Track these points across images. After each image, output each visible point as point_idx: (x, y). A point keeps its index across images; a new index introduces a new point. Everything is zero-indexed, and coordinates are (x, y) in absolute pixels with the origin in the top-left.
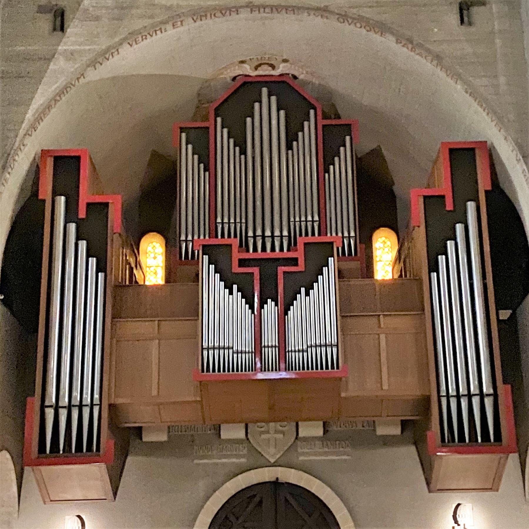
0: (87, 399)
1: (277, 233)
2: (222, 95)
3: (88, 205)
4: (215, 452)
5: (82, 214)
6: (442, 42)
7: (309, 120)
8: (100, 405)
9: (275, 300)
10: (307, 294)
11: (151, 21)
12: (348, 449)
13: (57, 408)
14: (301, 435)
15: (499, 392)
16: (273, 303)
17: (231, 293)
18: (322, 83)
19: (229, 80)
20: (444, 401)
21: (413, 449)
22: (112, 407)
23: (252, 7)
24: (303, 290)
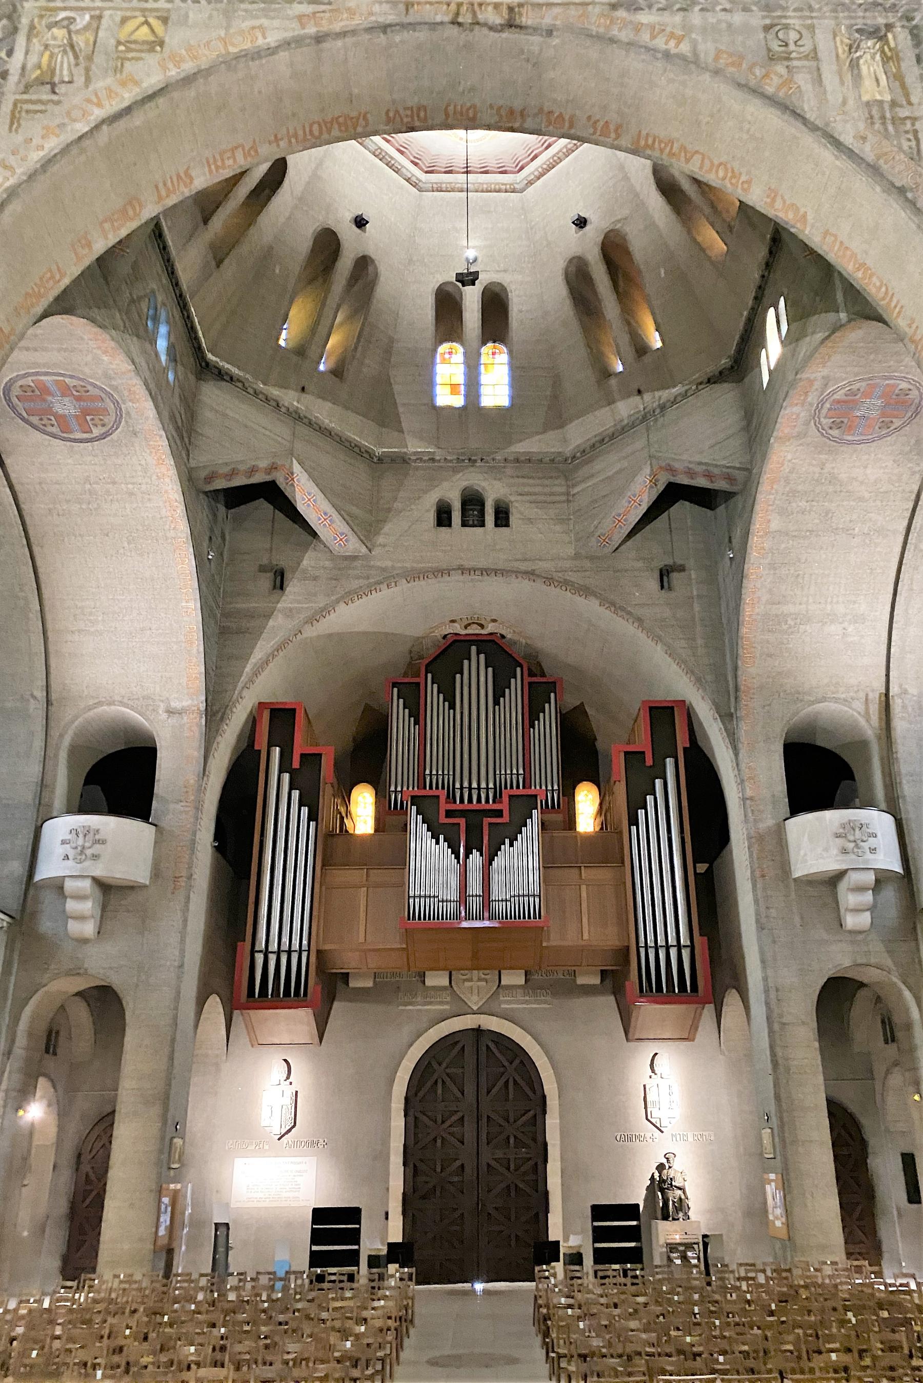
1: (483, 785)
2: (433, 652)
3: (302, 756)
4: (419, 999)
5: (296, 764)
6: (643, 605)
7: (515, 677)
8: (309, 951)
9: (480, 850)
10: (511, 845)
11: (366, 582)
12: (548, 998)
13: (266, 954)
14: (503, 983)
16: (478, 853)
17: (437, 843)
18: (529, 642)
19: (440, 638)
21: (612, 998)
23: (463, 570)
24: (507, 841)
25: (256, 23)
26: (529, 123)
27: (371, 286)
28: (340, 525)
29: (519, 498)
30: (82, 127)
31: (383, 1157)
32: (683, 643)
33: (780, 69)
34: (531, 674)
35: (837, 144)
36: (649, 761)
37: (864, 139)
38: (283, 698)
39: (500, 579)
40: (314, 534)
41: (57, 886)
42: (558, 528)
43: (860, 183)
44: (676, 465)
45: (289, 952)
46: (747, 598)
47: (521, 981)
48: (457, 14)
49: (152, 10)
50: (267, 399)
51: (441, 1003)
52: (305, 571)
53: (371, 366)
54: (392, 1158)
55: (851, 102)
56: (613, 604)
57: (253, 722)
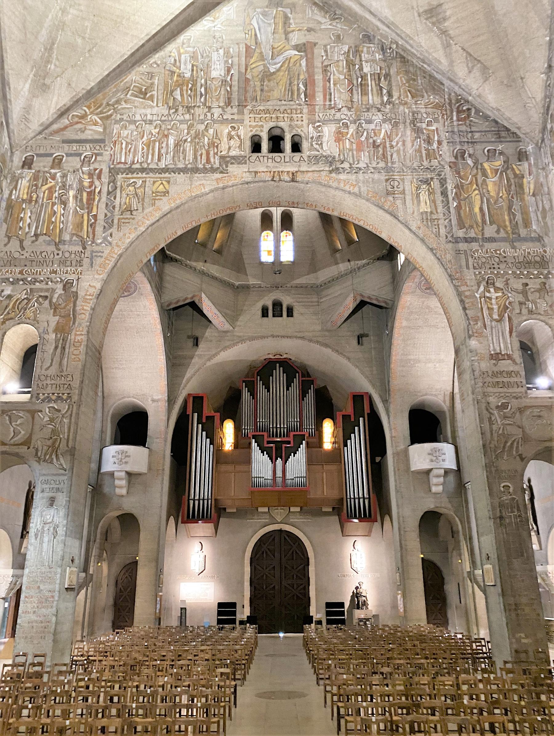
0: (206, 497)
1: (282, 426)
4: (256, 517)
5: (204, 421)
9: (281, 458)
20: (349, 500)
21: (337, 517)
22: (215, 500)
23: (273, 336)
25: (201, 182)
26: (300, 206)
28: (222, 319)
30: (143, 229)
31: (242, 583)
33: (391, 198)
34: (303, 376)
35: (410, 230)
36: (353, 420)
37: (420, 228)
39: (289, 339)
40: (210, 322)
42: (314, 317)
43: (419, 243)
44: (364, 294)
45: (203, 500)
46: (393, 353)
47: (298, 509)
48: (274, 177)
49: (164, 178)
51: (265, 519)
52: (207, 338)
53: (234, 247)
54: (245, 583)
55: (416, 213)
56: (337, 351)
57: (185, 402)
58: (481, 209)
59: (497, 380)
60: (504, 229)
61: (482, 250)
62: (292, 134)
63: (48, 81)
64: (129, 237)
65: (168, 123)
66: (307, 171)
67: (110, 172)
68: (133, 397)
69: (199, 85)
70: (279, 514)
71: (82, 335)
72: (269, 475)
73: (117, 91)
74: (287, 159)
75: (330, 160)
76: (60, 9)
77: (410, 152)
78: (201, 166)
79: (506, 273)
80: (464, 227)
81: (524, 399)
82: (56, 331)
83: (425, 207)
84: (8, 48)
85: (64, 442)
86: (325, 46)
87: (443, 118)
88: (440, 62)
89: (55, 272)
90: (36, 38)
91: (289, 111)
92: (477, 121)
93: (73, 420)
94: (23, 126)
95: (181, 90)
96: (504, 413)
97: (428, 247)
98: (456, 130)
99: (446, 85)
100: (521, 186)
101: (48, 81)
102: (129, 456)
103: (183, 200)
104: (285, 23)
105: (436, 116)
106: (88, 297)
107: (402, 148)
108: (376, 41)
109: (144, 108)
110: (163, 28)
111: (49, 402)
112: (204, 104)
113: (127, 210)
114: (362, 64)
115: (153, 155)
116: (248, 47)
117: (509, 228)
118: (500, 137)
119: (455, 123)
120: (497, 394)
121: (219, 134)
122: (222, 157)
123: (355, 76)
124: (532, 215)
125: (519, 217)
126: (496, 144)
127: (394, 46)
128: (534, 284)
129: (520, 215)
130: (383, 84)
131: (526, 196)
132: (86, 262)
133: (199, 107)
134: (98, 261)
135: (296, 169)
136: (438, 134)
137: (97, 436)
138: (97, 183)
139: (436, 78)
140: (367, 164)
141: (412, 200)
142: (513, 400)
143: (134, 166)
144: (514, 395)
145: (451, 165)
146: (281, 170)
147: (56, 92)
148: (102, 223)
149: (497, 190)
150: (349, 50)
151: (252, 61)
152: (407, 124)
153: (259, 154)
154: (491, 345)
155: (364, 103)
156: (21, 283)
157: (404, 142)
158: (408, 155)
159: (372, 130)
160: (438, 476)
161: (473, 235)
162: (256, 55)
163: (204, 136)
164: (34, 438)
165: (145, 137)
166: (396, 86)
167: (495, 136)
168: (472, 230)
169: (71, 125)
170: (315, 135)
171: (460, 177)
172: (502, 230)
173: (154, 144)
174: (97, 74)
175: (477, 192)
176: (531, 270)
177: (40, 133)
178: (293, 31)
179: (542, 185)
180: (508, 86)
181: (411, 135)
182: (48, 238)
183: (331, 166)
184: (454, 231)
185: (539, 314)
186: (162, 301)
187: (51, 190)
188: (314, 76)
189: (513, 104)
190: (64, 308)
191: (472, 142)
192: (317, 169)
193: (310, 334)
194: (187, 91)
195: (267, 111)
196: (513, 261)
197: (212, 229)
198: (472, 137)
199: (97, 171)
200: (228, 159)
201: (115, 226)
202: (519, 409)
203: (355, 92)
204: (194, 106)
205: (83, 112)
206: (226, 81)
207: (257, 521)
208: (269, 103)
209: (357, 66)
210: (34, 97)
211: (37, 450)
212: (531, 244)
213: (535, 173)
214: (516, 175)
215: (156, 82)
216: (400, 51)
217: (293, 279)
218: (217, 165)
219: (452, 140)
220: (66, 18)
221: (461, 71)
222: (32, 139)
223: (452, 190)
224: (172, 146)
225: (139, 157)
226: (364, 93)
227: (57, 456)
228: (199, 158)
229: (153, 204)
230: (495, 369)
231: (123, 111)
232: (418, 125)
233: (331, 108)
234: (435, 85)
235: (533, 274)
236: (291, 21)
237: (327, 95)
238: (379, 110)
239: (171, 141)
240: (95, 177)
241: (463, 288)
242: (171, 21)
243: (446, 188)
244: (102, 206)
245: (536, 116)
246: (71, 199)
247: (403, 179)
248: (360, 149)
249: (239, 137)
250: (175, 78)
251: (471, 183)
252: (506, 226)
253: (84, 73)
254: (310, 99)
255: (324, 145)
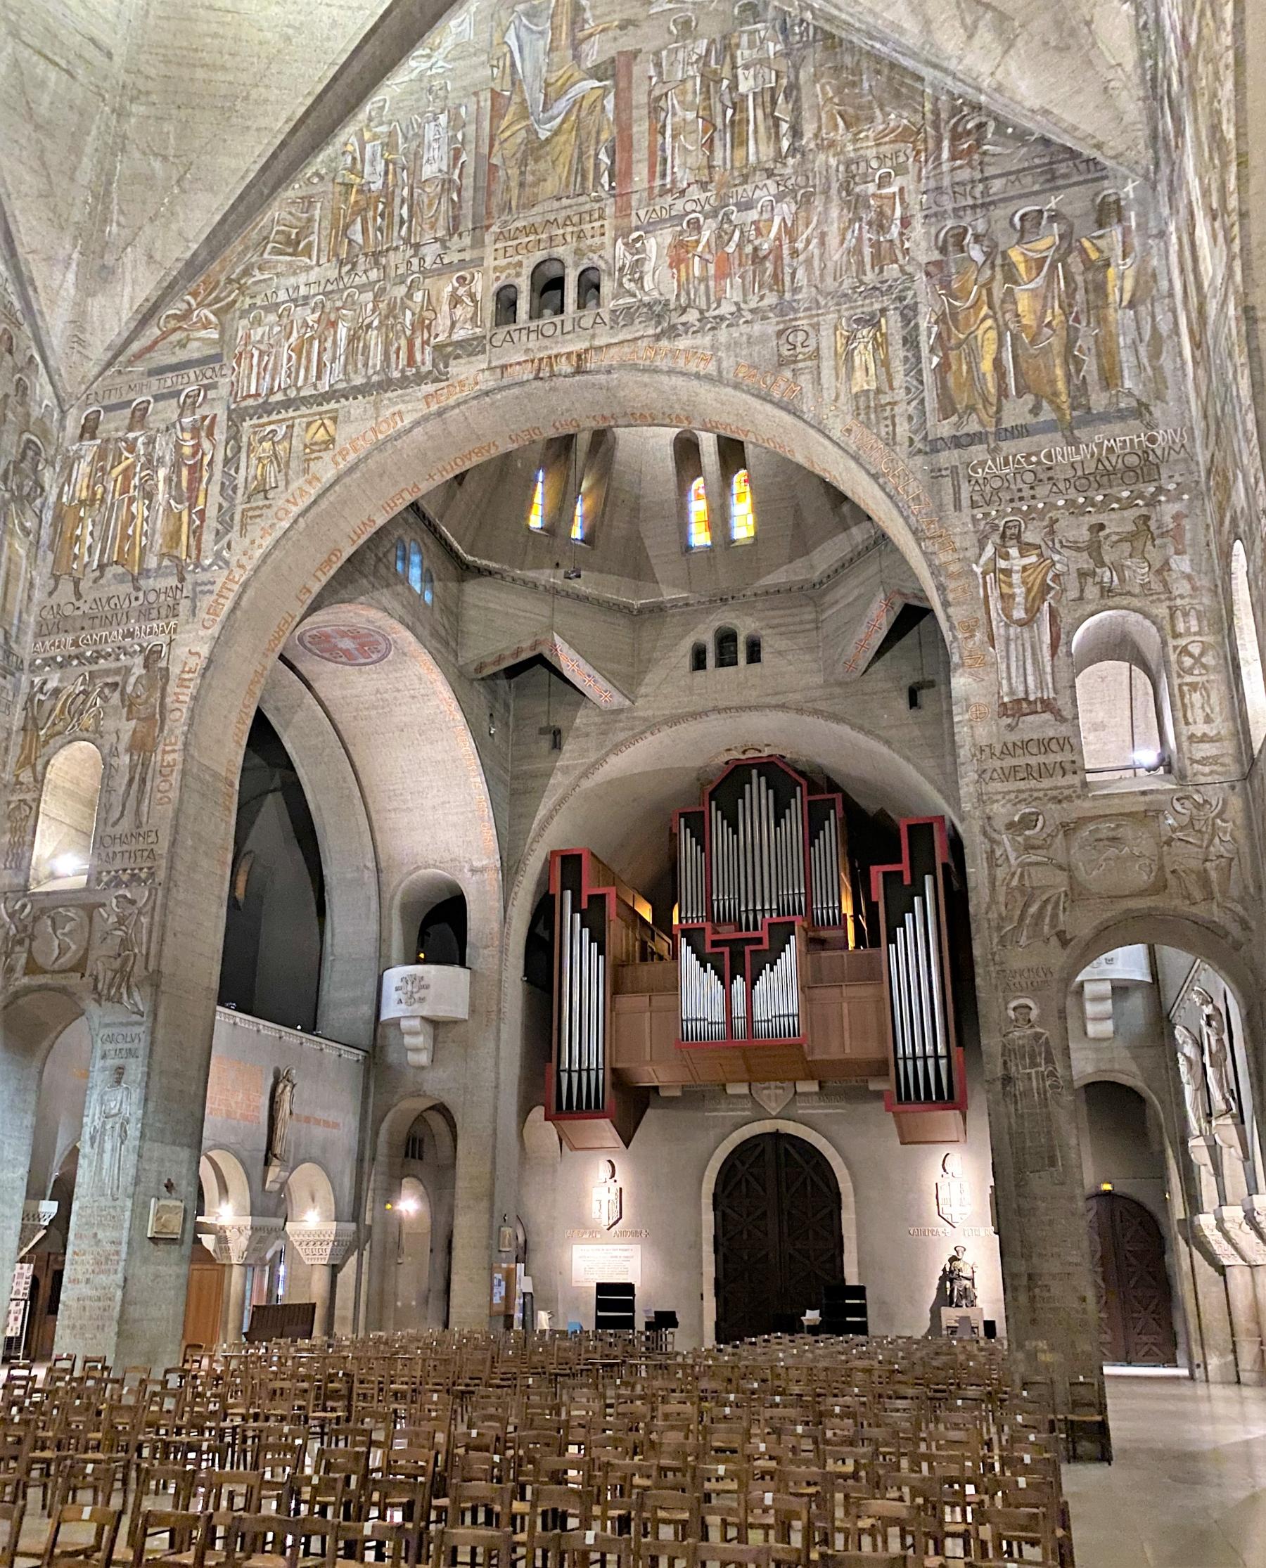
3: (591, 897)
5: (584, 905)
9: (743, 976)
15: (953, 1054)
27: (611, 450)
29: (769, 631)
32: (932, 762)
34: (813, 788)
38: (574, 844)
41: (396, 1023)
42: (807, 657)
45: (588, 1070)
47: (814, 1087)
50: (525, 583)
58: (998, 363)
59: (1015, 762)
60: (1051, 402)
61: (994, 460)
62: (581, 268)
63: (109, 259)
64: (260, 546)
65: (336, 296)
66: (609, 346)
67: (229, 419)
68: (435, 866)
69: (397, 201)
70: (773, 1097)
71: (174, 751)
72: (718, 1015)
73: (247, 248)
74: (568, 327)
75: (657, 312)
76: (113, 111)
77: (836, 257)
78: (396, 375)
79: (1052, 506)
80: (954, 411)
81: (1078, 802)
82: (130, 750)
83: (861, 382)
84: (17, 213)
85: (140, 962)
86: (657, 53)
87: (916, 160)
88: (902, 31)
89: (131, 634)
90: (72, 179)
91: (575, 219)
92: (998, 150)
93: (157, 918)
94: (76, 357)
95: (365, 222)
96: (1028, 838)
97: (868, 472)
98: (946, 182)
99: (928, 78)
100: (1100, 289)
101: (109, 259)
102: (427, 987)
103: (362, 454)
104: (573, 23)
105: (902, 159)
106: (186, 676)
107: (817, 252)
108: (771, 13)
109: (295, 273)
110: (320, 98)
111: (117, 886)
112: (407, 241)
113: (257, 491)
114: (735, 76)
115: (307, 369)
116: (495, 95)
117: (1064, 398)
118: (1053, 178)
119: (945, 167)
120: (1012, 796)
121: (434, 300)
122: (438, 348)
123: (719, 107)
124: (1126, 357)
125: (1090, 366)
126: (1042, 197)
127: (808, 16)
128: (1118, 523)
129: (1094, 362)
130: (783, 110)
131: (1111, 311)
132: (184, 606)
133: (397, 248)
134: (205, 602)
135: (586, 345)
136: (902, 200)
137: (370, 949)
138: (206, 445)
139: (905, 69)
140: (737, 304)
141: (836, 369)
142: (1050, 805)
143: (273, 399)
144: (1055, 793)
145: (931, 268)
146: (554, 352)
147: (128, 276)
148: (215, 524)
149: (1039, 308)
150: (708, 51)
151: (504, 123)
152: (834, 192)
153: (513, 327)
154: (1004, 682)
155: (737, 164)
156: (75, 662)
157: (823, 235)
158: (829, 264)
159: (753, 222)
160: (1098, 999)
161: (973, 426)
162: (512, 109)
163: (404, 307)
164: (92, 956)
165: (295, 334)
166: (811, 107)
167: (1042, 179)
168: (974, 416)
169: (165, 336)
170: (629, 259)
171: (951, 295)
172: (1045, 404)
173: (311, 345)
174: (200, 224)
175: (989, 322)
176: (1114, 491)
177: (109, 364)
178: (591, 35)
179: (1154, 276)
180: (1062, 49)
181: (840, 217)
182: (120, 570)
183: (659, 323)
184: (929, 424)
185: (1129, 593)
186: (461, 663)
187: (127, 474)
188: (630, 127)
189: (1079, 92)
190: (146, 702)
191: (983, 205)
192: (629, 337)
193: (798, 696)
194: (375, 219)
195: (532, 229)
196: (1070, 473)
197: (565, 494)
198: (985, 193)
199: (207, 422)
200: (450, 349)
201: (237, 528)
202: (1063, 825)
203: (717, 143)
204: (388, 250)
205: (185, 306)
206: (450, 181)
207: (725, 1113)
208: (535, 210)
209: (725, 83)
210: (88, 295)
211: (96, 980)
212: (1117, 427)
213: (1138, 248)
214: (1088, 264)
215: (317, 213)
216: (821, 23)
217: (759, 577)
218: (428, 366)
219: (935, 209)
220: (126, 126)
221: (949, 40)
222: (96, 378)
223: (929, 329)
224: (343, 344)
225: (282, 379)
226: (739, 141)
227: (128, 988)
228: (393, 357)
229: (306, 471)
230: (1011, 738)
231: (256, 288)
232: (857, 189)
233: (664, 192)
234: (902, 84)
235: (1118, 500)
236: (588, 15)
237: (657, 162)
238: (770, 174)
239: (342, 332)
240: (203, 434)
241: (943, 557)
242: (335, 79)
243: (917, 326)
244: (215, 489)
245: (1131, 105)
246: (161, 485)
247: (818, 324)
248: (722, 275)
249: (472, 296)
250: (352, 199)
251: (976, 305)
252: (1056, 394)
253: (174, 227)
254: (620, 184)
255: (648, 280)
